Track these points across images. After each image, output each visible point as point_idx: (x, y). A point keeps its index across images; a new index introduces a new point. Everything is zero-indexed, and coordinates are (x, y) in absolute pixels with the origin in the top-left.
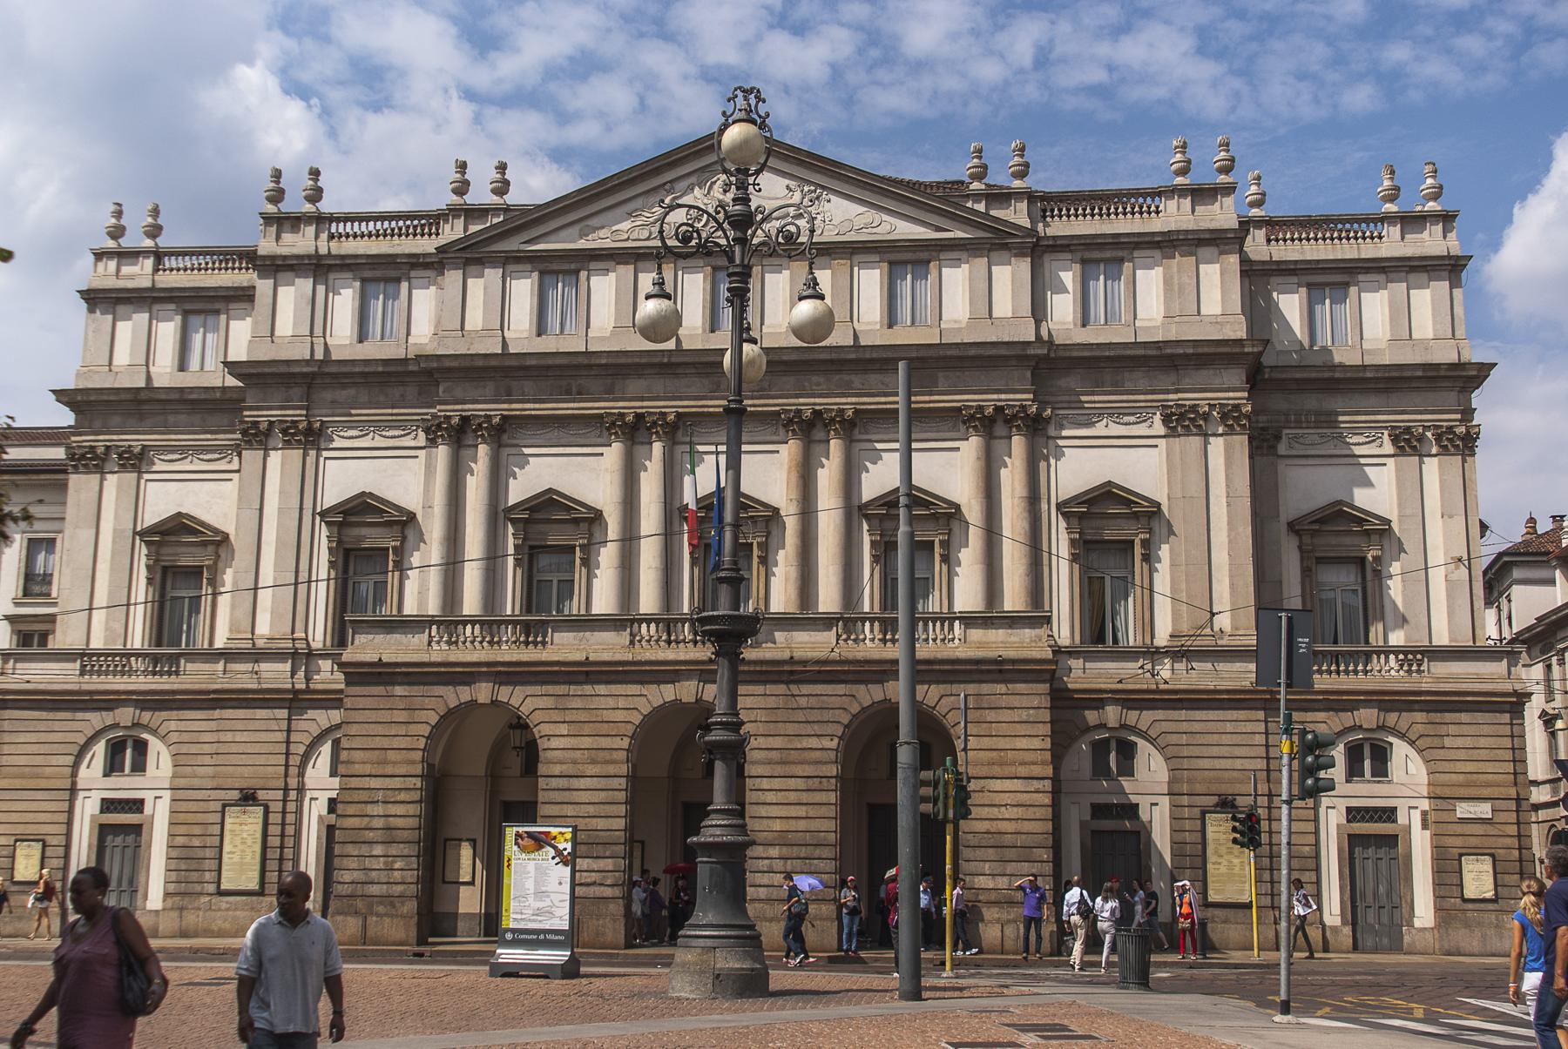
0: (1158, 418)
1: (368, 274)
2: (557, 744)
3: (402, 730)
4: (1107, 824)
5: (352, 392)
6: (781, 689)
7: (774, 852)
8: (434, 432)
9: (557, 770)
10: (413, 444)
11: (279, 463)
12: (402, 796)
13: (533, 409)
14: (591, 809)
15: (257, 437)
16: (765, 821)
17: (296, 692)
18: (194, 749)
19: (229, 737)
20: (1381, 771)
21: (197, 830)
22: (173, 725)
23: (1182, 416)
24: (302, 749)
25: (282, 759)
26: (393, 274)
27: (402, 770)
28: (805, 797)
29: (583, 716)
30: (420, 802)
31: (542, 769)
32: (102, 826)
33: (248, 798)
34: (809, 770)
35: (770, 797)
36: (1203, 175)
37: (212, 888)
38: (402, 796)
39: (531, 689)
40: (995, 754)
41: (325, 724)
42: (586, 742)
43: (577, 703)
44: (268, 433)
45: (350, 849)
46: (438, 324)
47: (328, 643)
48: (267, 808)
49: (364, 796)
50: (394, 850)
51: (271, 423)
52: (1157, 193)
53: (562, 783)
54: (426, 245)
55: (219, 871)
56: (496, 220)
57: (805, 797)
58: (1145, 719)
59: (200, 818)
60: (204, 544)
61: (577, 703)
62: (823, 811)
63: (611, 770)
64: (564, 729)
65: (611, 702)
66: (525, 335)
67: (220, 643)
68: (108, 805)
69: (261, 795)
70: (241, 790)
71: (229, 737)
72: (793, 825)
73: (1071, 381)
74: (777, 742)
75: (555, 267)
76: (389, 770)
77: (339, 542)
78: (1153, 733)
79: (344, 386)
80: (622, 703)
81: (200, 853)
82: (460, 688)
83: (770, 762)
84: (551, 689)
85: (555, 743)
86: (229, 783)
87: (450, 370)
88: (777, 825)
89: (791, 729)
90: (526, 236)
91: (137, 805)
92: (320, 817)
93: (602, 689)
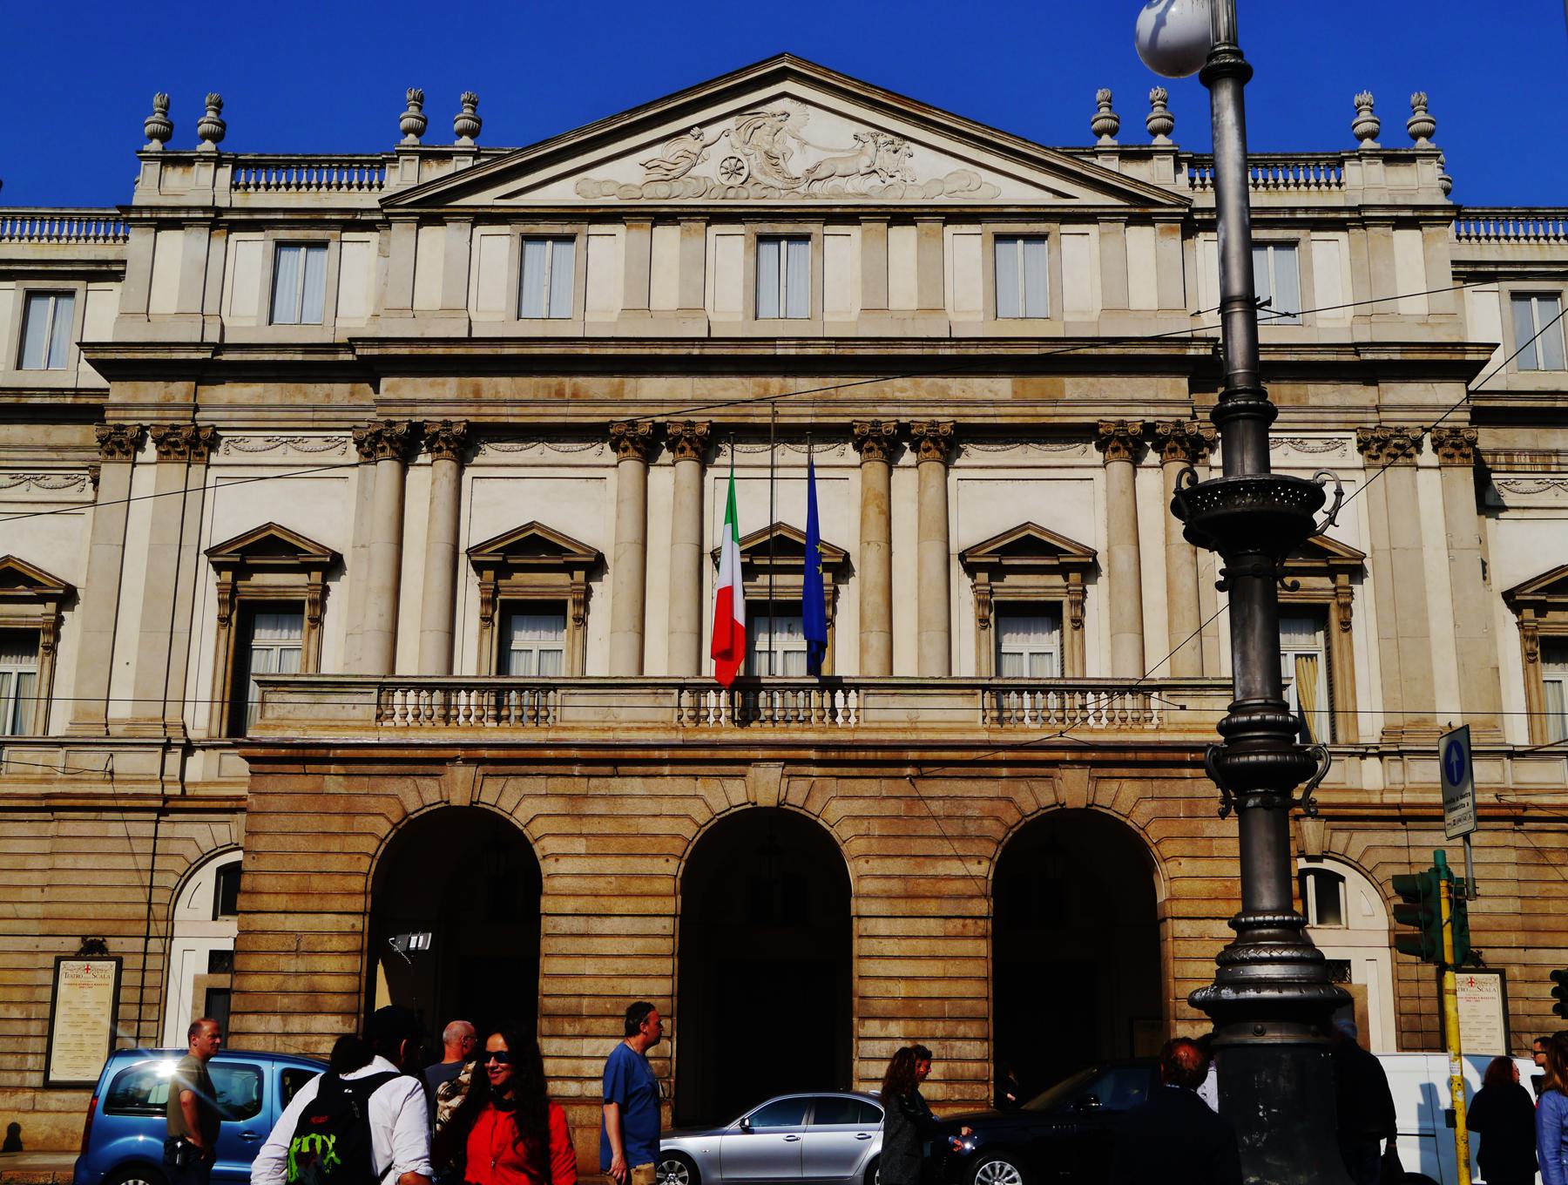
0: (1352, 445)
1: (284, 234)
2: (565, 867)
3: (335, 844)
6: (903, 788)
8: (371, 446)
9: (570, 905)
10: (341, 461)
11: (150, 475)
12: (336, 944)
13: (510, 415)
14: (622, 965)
15: (122, 445)
16: (883, 984)
17: (166, 798)
18: (17, 879)
19: (68, 862)
21: (17, 995)
23: (1383, 443)
24: (172, 881)
25: (141, 896)
27: (338, 903)
28: (941, 947)
29: (608, 827)
30: (360, 952)
31: (546, 904)
33: (93, 949)
34: (948, 908)
35: (890, 947)
37: (36, 1079)
38: (336, 944)
39: (529, 785)
40: (1218, 885)
41: (207, 845)
42: (612, 865)
43: (599, 807)
44: (139, 444)
45: (252, 1022)
46: (381, 297)
47: (215, 732)
48: (120, 962)
49: (275, 943)
51: (143, 429)
53: (578, 925)
54: (367, 199)
55: (48, 1054)
56: (462, 166)
57: (941, 947)
58: (1359, 841)
59: (23, 977)
60: (41, 599)
61: (599, 807)
62: (971, 968)
63: (652, 905)
64: (580, 846)
65: (651, 807)
66: (500, 317)
67: (58, 729)
69: (113, 945)
70: (84, 937)
71: (68, 862)
72: (925, 989)
75: (543, 228)
76: (314, 904)
77: (234, 591)
78: (1367, 864)
80: (667, 807)
81: (19, 1028)
82: (427, 781)
83: (890, 897)
84: (559, 785)
85: (565, 866)
86: (67, 927)
88: (901, 989)
89: (918, 847)
92: (197, 979)
93: (636, 786)
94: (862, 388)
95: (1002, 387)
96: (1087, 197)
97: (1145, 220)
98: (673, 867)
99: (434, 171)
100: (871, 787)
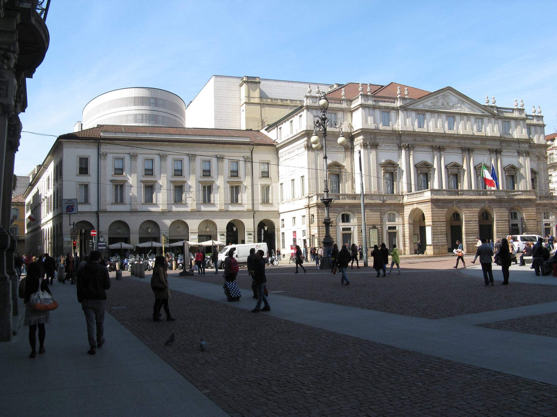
3: (441, 212)
4: (514, 228)
5: (382, 137)
7: (500, 234)
20: (548, 218)
22: (356, 211)
26: (388, 111)
32: (343, 234)
33: (374, 227)
36: (519, 107)
38: (443, 225)
42: (471, 214)
50: (442, 236)
52: (513, 109)
64: (468, 212)
68: (344, 229)
73: (504, 145)
74: (499, 214)
79: (382, 135)
85: (467, 214)
87: (405, 134)
90: (413, 105)
91: (349, 229)
92: (387, 231)
94: (463, 141)
95: (479, 142)
96: (487, 113)
97: (494, 117)
98: (477, 214)
99: (405, 102)
100: (496, 204)
